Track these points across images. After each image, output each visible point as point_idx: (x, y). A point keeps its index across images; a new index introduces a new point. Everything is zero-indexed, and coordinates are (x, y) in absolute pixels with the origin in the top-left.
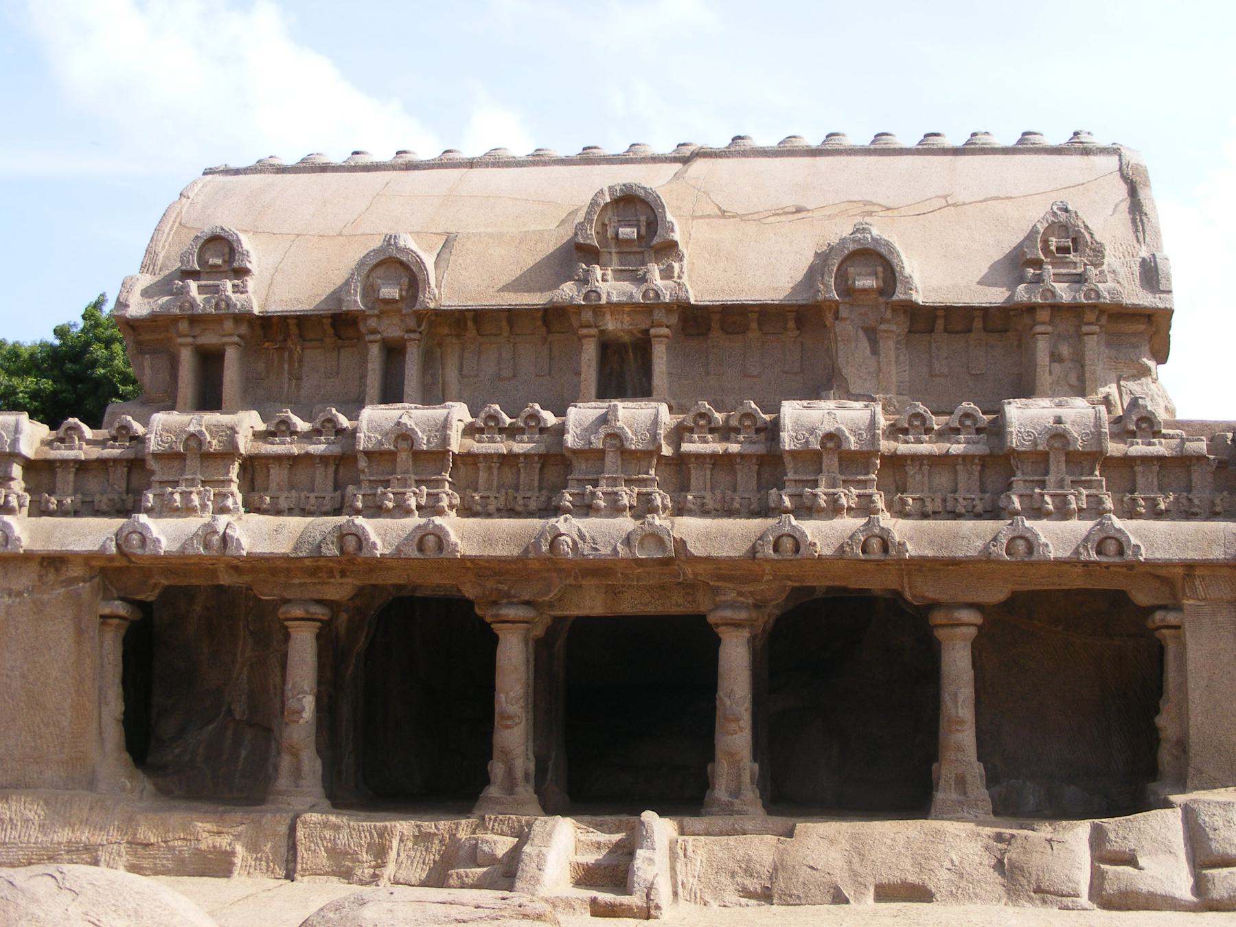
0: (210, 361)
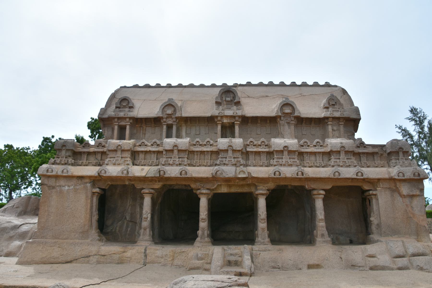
0: (122, 129)
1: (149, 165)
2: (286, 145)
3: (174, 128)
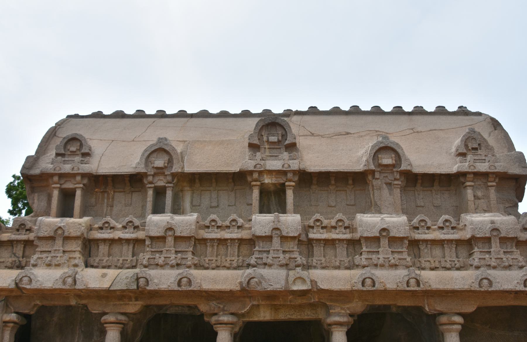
0: (67, 196)
1: (116, 267)
2: (385, 226)
3: (169, 194)
